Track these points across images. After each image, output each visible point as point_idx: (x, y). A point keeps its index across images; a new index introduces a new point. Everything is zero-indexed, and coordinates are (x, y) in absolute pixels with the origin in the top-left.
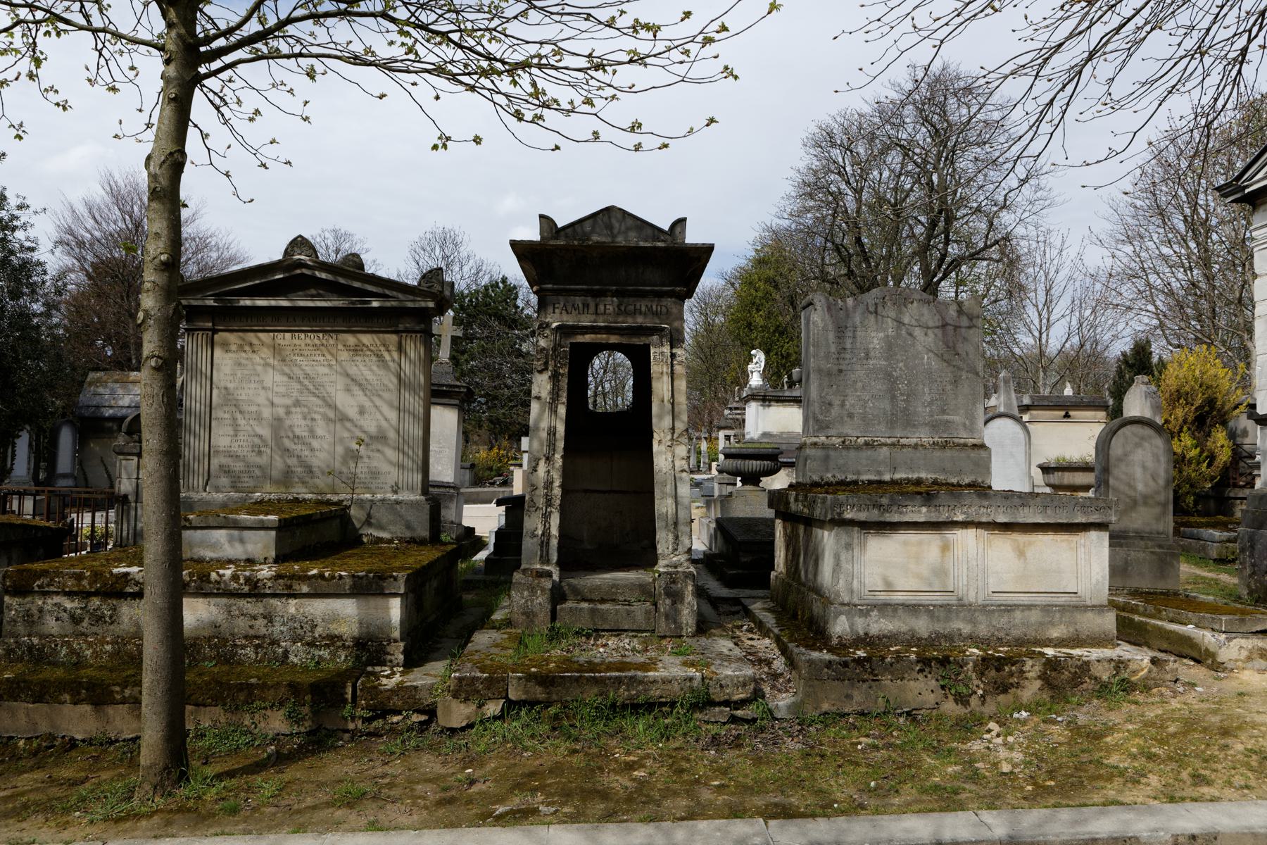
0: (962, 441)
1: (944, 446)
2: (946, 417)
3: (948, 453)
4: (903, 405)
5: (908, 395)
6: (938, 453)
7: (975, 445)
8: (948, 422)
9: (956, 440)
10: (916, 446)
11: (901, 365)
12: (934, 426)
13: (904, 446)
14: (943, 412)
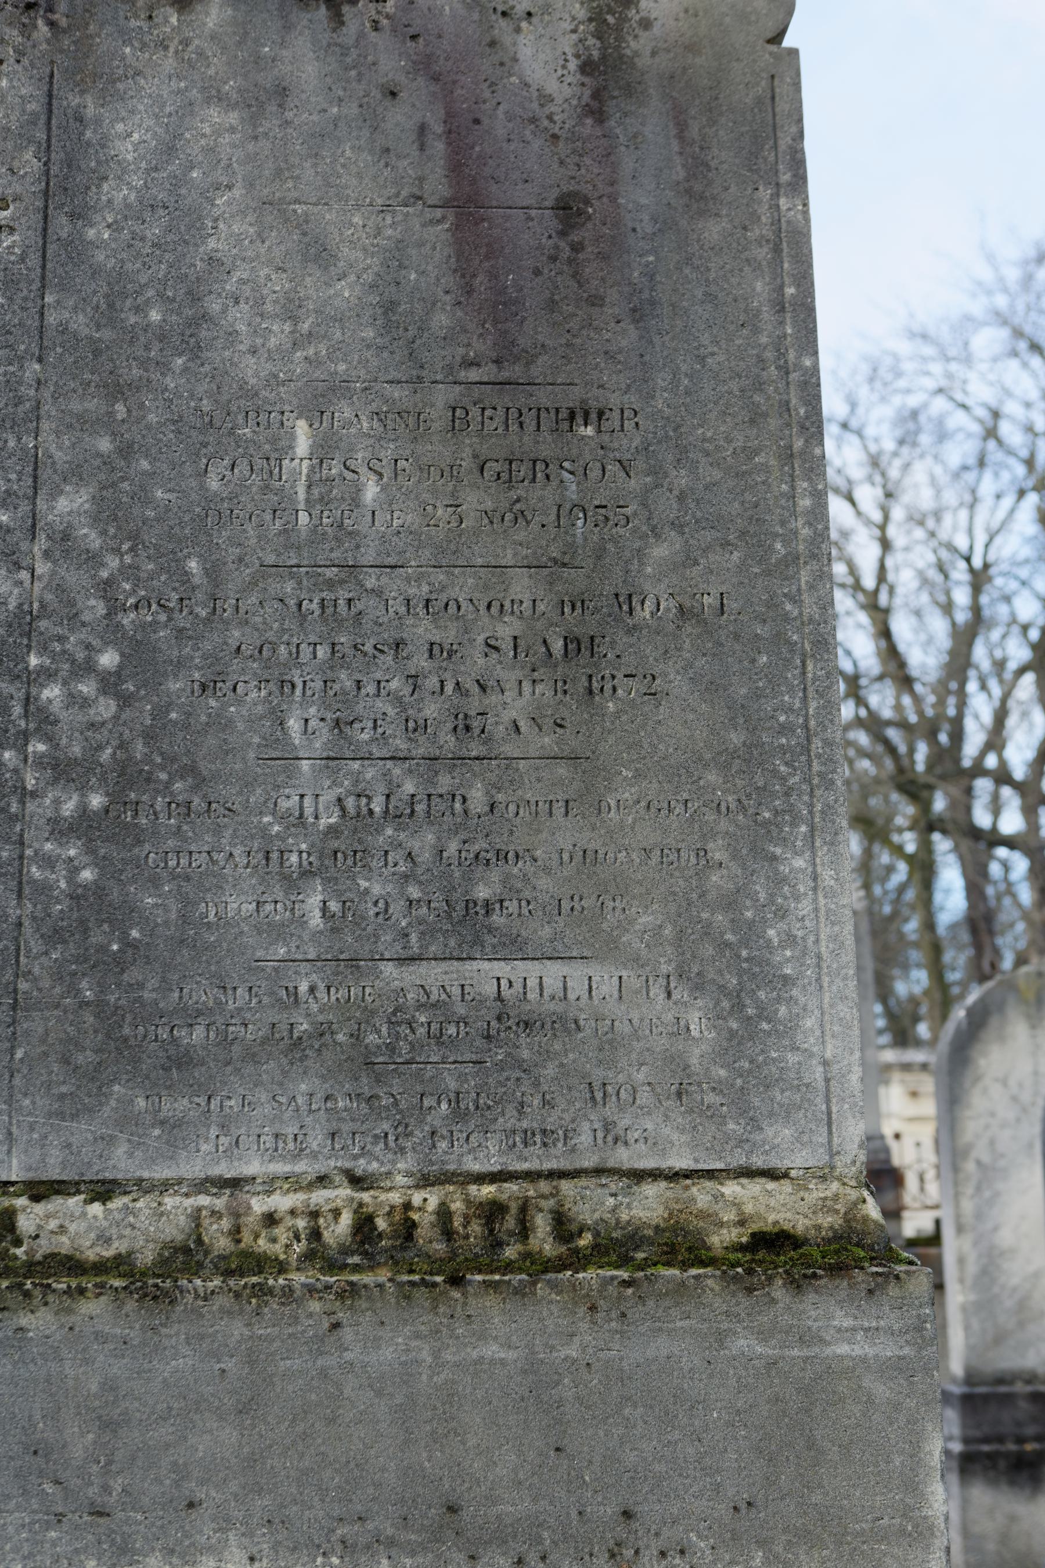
0: (648, 1206)
1: (478, 1252)
2: (485, 974)
3: (497, 1336)
4: (67, 867)
5: (126, 778)
6: (388, 1344)
7: (770, 1246)
8: (510, 1020)
9: (593, 1204)
10: (157, 1280)
11: (69, 504)
12: (380, 1065)
13: (69, 1271)
14: (469, 926)
